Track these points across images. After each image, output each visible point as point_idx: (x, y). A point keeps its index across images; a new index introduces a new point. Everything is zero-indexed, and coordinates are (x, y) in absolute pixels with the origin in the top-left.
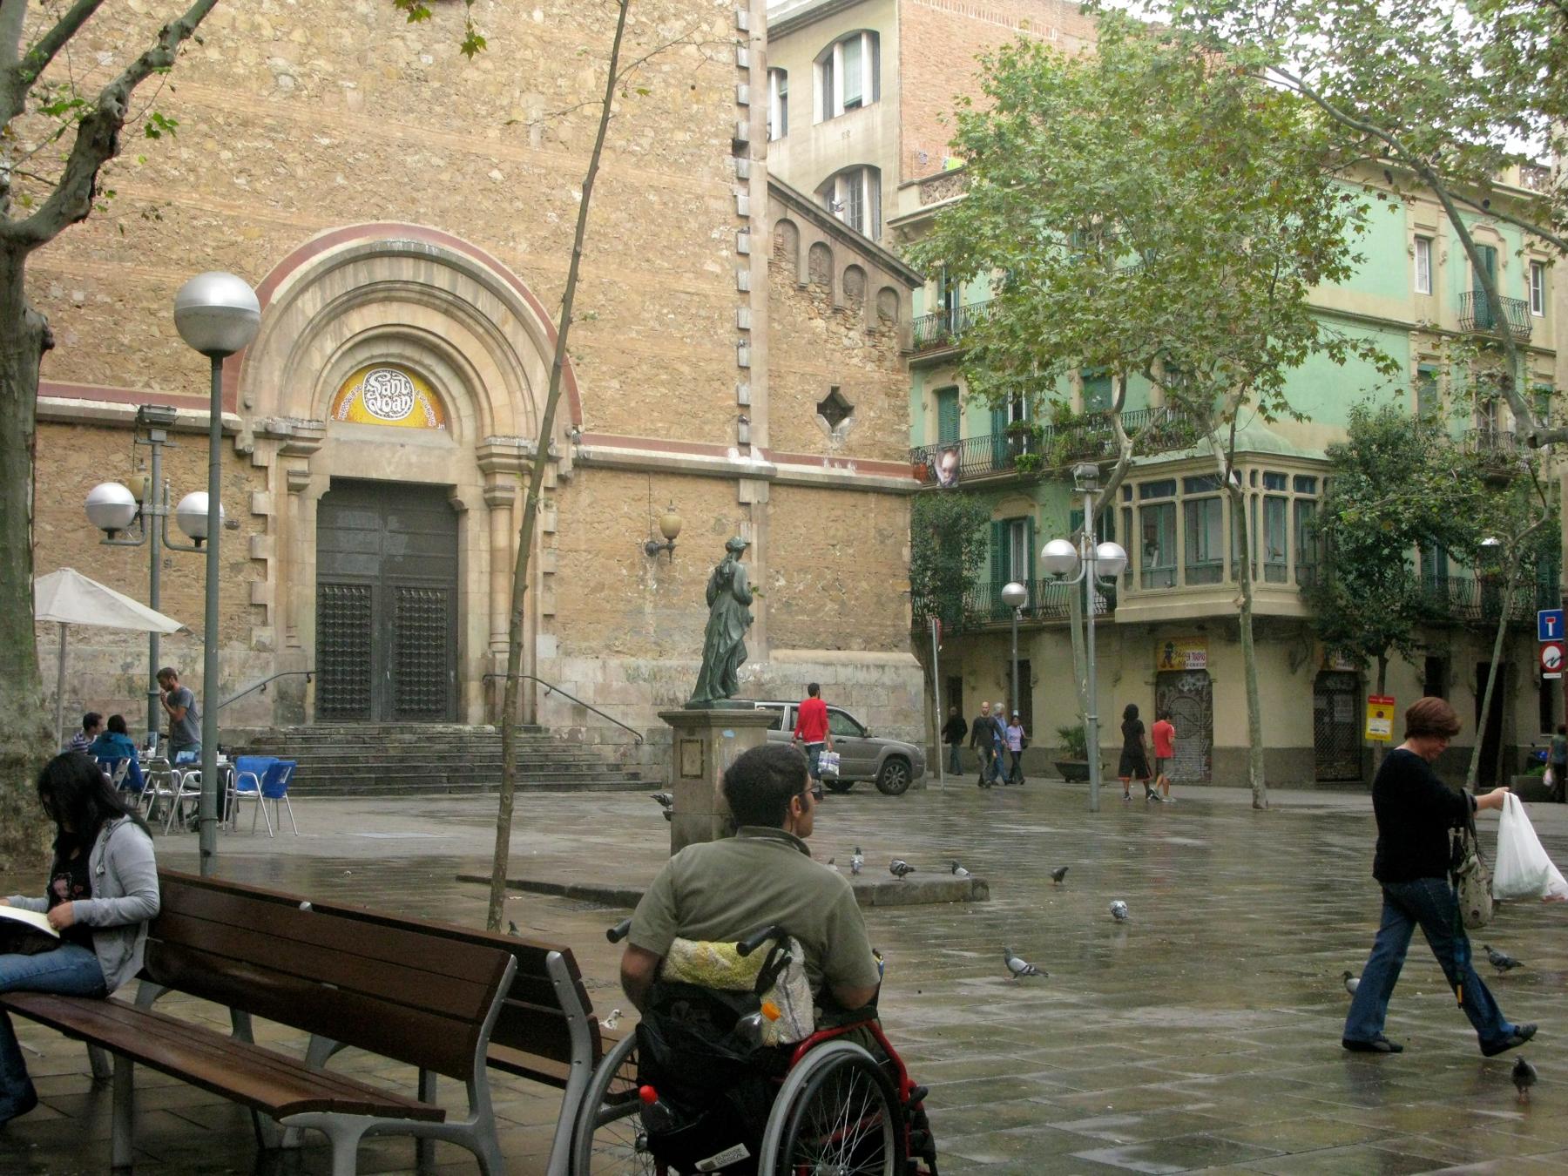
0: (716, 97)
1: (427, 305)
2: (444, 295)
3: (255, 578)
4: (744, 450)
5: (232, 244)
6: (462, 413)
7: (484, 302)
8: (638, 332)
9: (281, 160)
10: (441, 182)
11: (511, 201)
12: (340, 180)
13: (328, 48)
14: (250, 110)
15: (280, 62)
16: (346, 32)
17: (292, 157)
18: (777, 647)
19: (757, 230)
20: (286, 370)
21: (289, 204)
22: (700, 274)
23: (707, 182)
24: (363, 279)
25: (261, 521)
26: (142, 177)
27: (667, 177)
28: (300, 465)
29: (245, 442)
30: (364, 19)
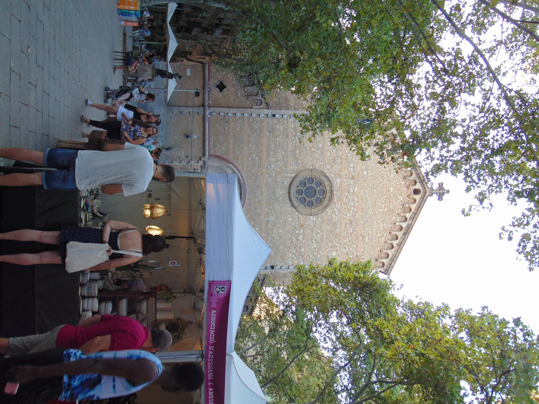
0: (282, 261)
9: (255, 166)
15: (272, 166)
20: (217, 167)
21: (247, 168)
26: (248, 140)
29: (203, 159)
30: (283, 183)
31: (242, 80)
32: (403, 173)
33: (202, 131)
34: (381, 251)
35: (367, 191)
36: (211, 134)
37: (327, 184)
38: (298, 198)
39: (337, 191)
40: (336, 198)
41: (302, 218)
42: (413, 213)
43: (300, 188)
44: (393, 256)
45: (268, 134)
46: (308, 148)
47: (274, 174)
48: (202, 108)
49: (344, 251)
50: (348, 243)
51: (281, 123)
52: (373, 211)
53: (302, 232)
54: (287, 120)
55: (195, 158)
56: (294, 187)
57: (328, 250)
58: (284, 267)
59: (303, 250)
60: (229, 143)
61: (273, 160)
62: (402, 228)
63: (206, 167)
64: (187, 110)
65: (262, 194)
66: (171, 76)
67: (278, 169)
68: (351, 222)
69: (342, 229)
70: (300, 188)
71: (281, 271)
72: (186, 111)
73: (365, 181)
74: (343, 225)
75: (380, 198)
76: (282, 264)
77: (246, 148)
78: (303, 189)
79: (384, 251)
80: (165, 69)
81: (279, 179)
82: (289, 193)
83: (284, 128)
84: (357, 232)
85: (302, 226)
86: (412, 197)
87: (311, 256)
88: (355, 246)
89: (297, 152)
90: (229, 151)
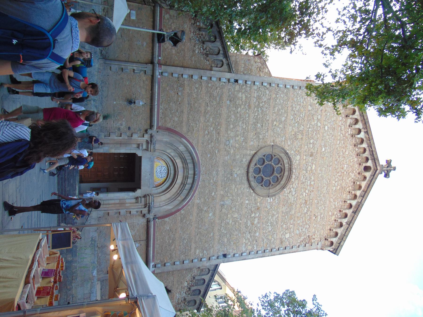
0: (235, 248)
1: (183, 178)
2: (186, 182)
3: (116, 134)
4: (154, 266)
5: (193, 130)
6: (158, 190)
7: (185, 192)
8: (181, 233)
9: (212, 142)
10: (210, 180)
11: (208, 198)
12: (209, 156)
13: (235, 152)
14: (221, 134)
15: (231, 141)
16: (239, 156)
17: (212, 143)
18: (101, 284)
19: (207, 263)
20: (166, 142)
21: (203, 144)
22: (196, 248)
23: (216, 248)
24: (188, 161)
25: (131, 136)
26: (205, 110)
28: (144, 147)
29: (150, 132)
30: (242, 161)
31: (201, 33)
32: (357, 150)
33: (149, 96)
34: (330, 230)
36: (161, 100)
37: (286, 161)
38: (255, 177)
40: (294, 176)
41: (259, 200)
42: (363, 191)
43: (258, 166)
44: (341, 234)
45: (228, 102)
46: (270, 121)
47: (232, 151)
48: (150, 66)
49: (298, 232)
50: (301, 224)
51: (243, 91)
52: (327, 189)
53: (257, 215)
54: (250, 87)
55: (140, 130)
56: (252, 165)
57: (282, 233)
58: (237, 255)
59: (257, 234)
60: (182, 112)
61: (232, 134)
62: (351, 206)
63: (153, 141)
64: (130, 67)
65: (217, 174)
67: (237, 145)
68: (306, 202)
69: (297, 209)
70: (258, 166)
72: (129, 67)
73: (323, 158)
74: (298, 206)
75: (334, 176)
76: (235, 252)
77: (202, 119)
82: (248, 172)
83: (246, 97)
84: (311, 212)
85: (258, 209)
87: (265, 240)
88: (308, 227)
89: (259, 125)
90: (182, 122)
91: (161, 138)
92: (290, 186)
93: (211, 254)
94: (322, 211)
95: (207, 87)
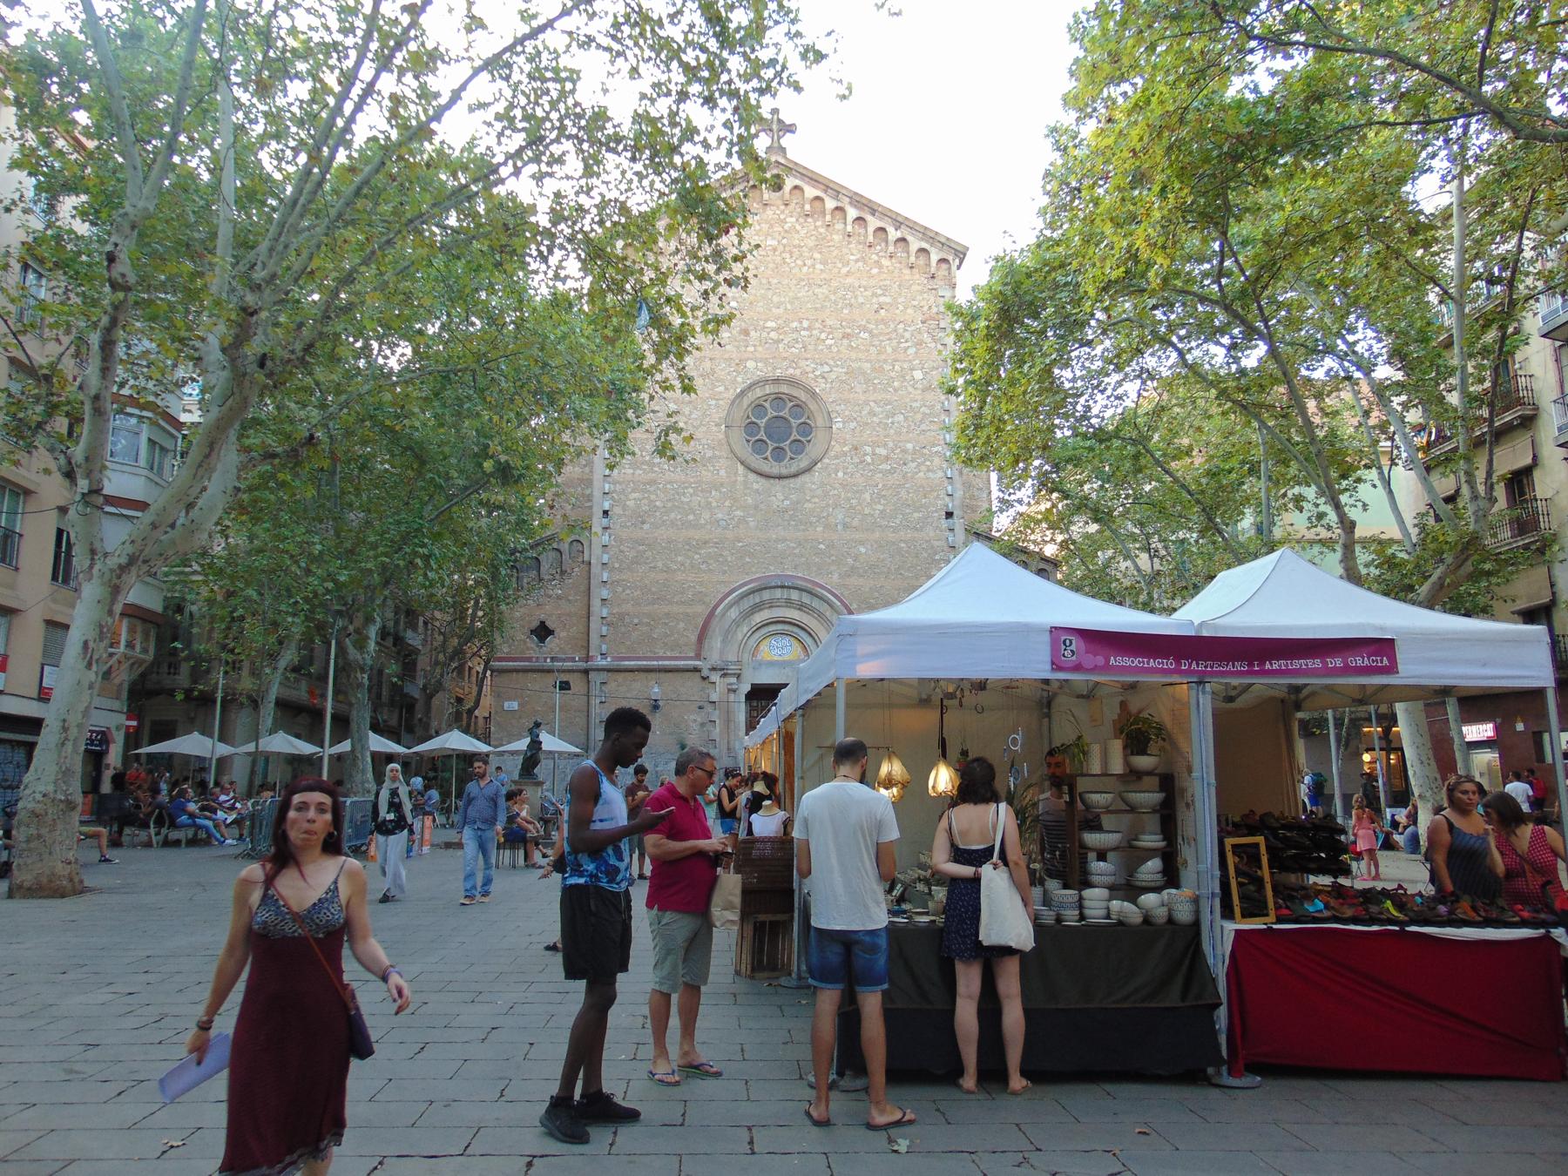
7: (816, 603)
23: (932, 534)
27: (910, 534)
28: (734, 680)
33: (643, 675)
35: (775, 299)
37: (759, 392)
39: (775, 368)
40: (791, 371)
41: (837, 448)
45: (646, 526)
47: (738, 513)
48: (592, 675)
49: (911, 351)
53: (868, 449)
56: (765, 467)
59: (909, 446)
60: (667, 615)
61: (706, 515)
66: (536, 744)
68: (846, 336)
71: (959, 494)
74: (854, 355)
76: (942, 494)
77: (680, 576)
78: (771, 445)
79: (912, 259)
80: (520, 759)
81: (750, 501)
82: (780, 477)
83: (633, 491)
86: (787, 196)
87: (923, 427)
91: (716, 651)
92: (809, 380)
93: (943, 543)
94: (868, 293)
95: (620, 570)
